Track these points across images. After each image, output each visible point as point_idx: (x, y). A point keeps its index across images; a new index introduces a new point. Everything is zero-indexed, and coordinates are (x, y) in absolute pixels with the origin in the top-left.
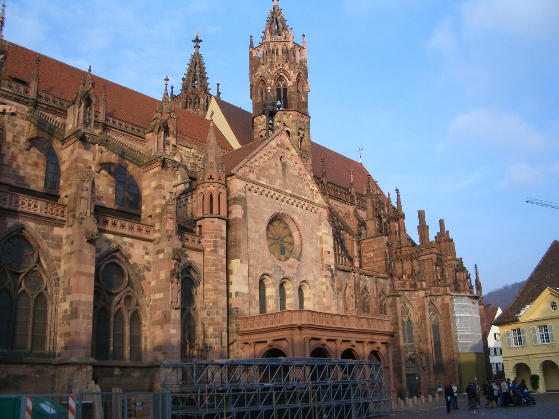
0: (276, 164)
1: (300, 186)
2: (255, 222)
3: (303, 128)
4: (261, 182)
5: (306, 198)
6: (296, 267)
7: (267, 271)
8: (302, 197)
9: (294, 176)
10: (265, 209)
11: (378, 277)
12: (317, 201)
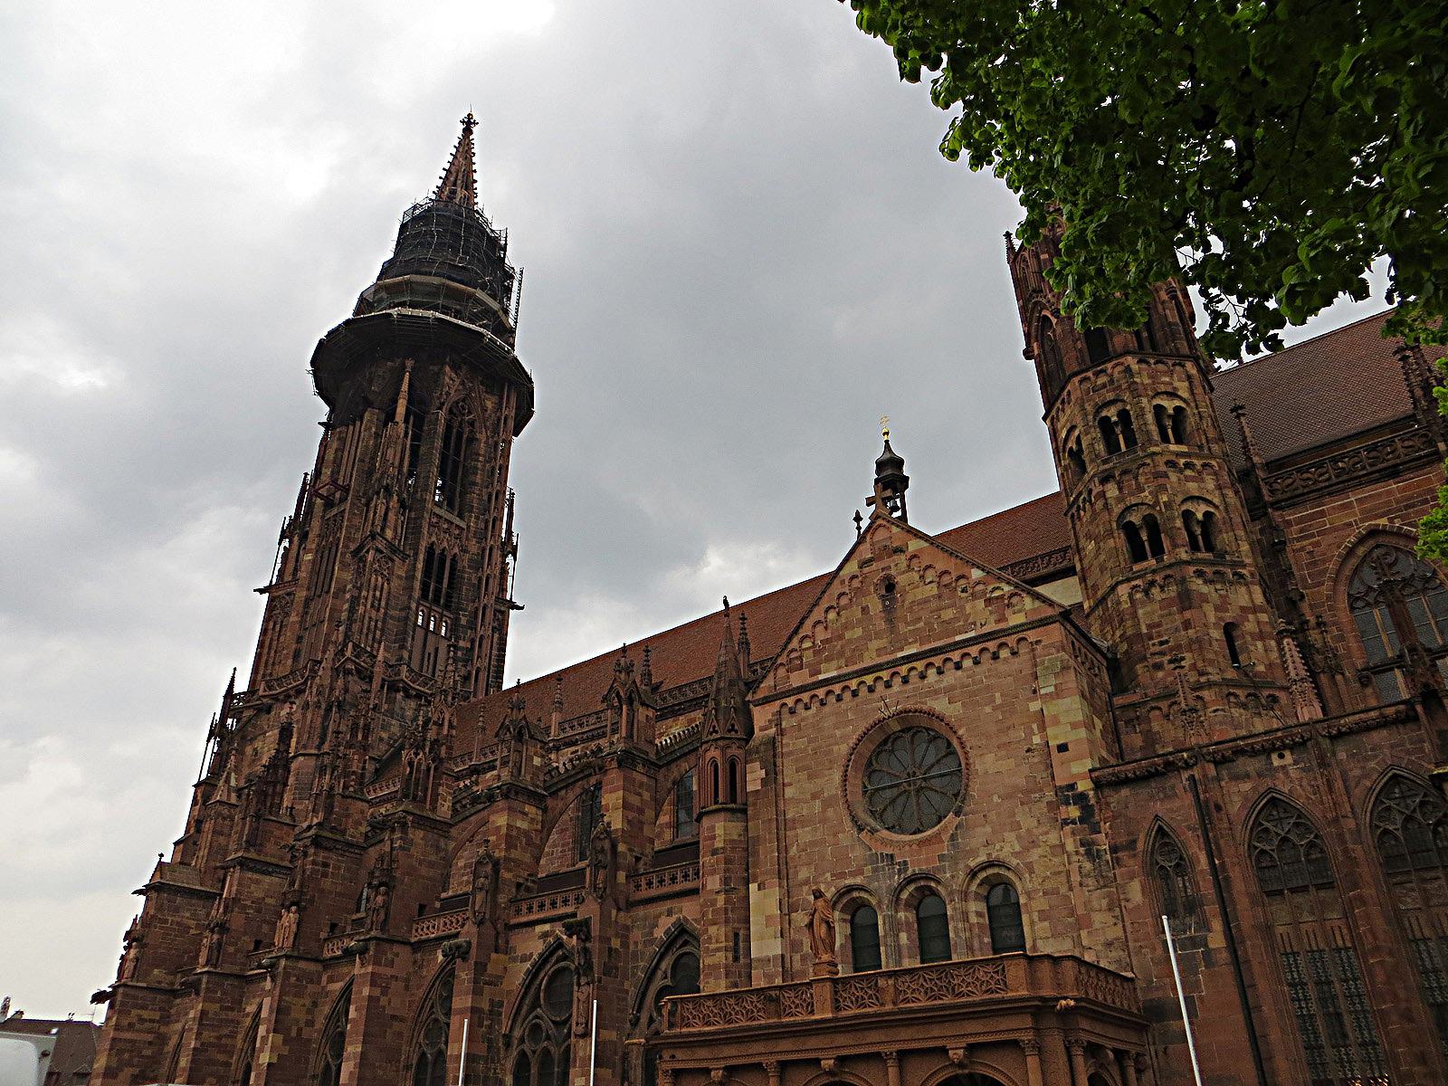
0: (865, 610)
1: (948, 614)
2: (810, 777)
3: (1110, 396)
4: (821, 677)
5: (972, 634)
6: (945, 837)
7: (848, 882)
8: (958, 638)
9: (926, 601)
10: (838, 733)
11: (1341, 735)
12: (1016, 619)
